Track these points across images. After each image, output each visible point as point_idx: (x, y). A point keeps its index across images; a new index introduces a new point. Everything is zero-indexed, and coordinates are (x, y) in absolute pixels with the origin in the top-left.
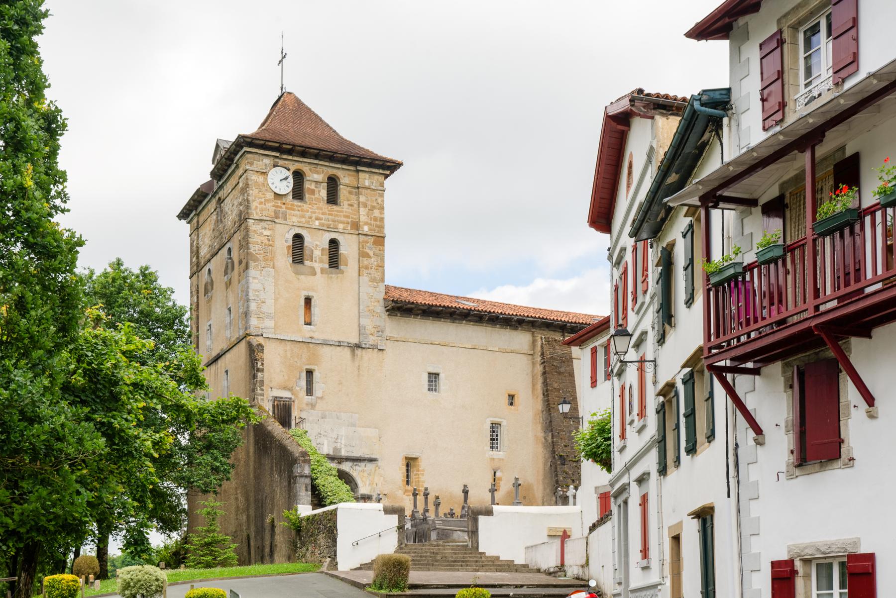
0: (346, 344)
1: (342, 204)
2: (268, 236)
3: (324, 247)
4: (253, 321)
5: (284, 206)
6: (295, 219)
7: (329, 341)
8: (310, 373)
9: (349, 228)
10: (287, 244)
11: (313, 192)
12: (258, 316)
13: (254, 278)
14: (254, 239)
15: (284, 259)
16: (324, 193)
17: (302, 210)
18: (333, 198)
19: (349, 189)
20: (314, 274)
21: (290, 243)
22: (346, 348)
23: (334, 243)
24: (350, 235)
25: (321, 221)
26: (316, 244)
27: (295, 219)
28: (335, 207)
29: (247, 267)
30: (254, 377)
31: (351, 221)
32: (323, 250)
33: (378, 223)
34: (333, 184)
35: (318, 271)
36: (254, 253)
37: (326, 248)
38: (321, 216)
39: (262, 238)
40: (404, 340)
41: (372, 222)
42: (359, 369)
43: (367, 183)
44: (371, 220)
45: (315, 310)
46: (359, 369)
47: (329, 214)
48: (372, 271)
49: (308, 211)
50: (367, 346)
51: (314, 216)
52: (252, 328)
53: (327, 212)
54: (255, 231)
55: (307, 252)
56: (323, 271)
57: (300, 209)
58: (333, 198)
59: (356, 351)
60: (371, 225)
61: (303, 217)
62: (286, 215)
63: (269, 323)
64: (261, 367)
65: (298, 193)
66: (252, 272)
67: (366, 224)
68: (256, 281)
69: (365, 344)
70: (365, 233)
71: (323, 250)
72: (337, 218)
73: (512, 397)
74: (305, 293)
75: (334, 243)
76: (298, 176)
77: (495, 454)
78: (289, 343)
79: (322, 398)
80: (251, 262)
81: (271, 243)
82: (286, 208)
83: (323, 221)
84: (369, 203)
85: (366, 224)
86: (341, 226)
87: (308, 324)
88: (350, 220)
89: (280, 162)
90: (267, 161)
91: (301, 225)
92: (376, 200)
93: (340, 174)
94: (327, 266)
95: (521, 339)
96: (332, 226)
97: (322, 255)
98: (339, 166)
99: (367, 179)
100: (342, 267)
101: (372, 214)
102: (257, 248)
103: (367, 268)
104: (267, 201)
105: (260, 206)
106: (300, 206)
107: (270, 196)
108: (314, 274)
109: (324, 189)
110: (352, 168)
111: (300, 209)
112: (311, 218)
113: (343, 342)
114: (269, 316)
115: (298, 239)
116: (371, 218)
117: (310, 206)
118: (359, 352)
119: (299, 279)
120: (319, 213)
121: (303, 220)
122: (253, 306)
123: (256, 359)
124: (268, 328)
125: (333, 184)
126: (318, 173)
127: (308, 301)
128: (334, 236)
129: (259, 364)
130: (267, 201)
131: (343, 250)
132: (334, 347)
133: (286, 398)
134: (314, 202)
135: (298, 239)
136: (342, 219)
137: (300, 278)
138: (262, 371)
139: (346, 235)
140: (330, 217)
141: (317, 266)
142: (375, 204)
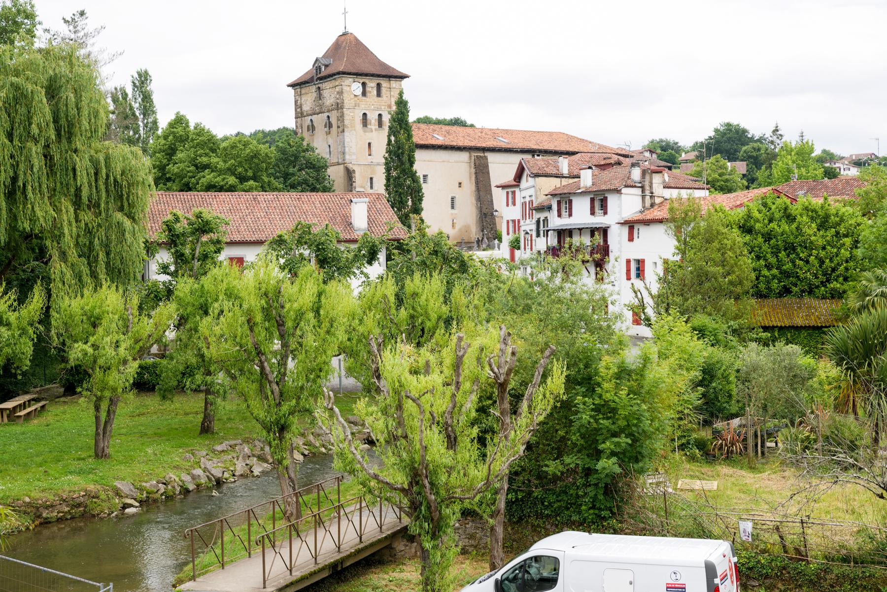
4: (347, 157)
8: (371, 179)
11: (370, 92)
14: (346, 118)
16: (375, 92)
18: (379, 94)
20: (372, 131)
23: (380, 115)
26: (373, 117)
27: (363, 106)
29: (343, 131)
30: (352, 185)
34: (379, 86)
43: (394, 86)
45: (373, 148)
56: (376, 130)
58: (379, 94)
63: (354, 157)
65: (364, 94)
66: (346, 134)
73: (460, 184)
74: (369, 141)
75: (380, 115)
76: (364, 84)
77: (453, 211)
86: (383, 107)
87: (370, 155)
89: (356, 80)
90: (351, 80)
95: (464, 156)
99: (394, 84)
104: (351, 99)
107: (352, 96)
108: (372, 131)
115: (365, 114)
122: (347, 149)
125: (379, 86)
127: (369, 144)
128: (380, 112)
130: (351, 99)
135: (365, 114)
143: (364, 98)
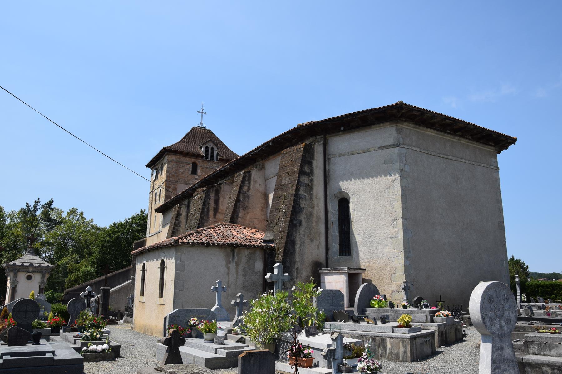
98: (161, 159)
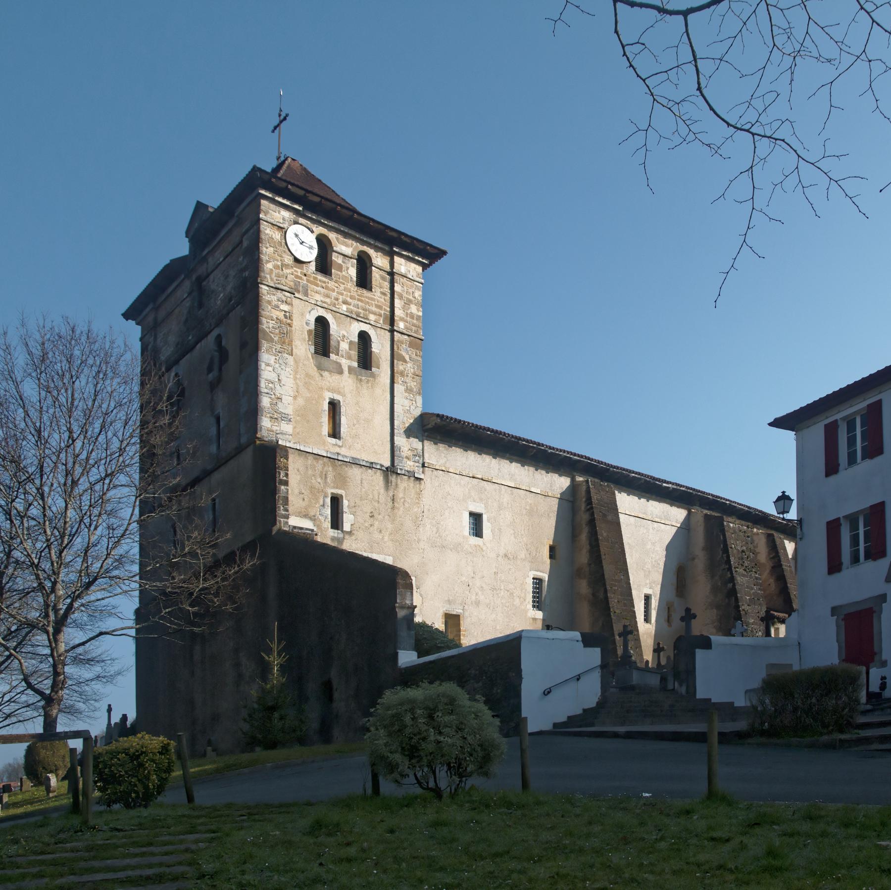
0: (378, 467)
1: (373, 290)
2: (285, 312)
3: (353, 340)
5: (305, 278)
6: (318, 297)
7: (358, 459)
9: (381, 322)
10: (308, 328)
12: (272, 415)
13: (268, 365)
15: (304, 348)
16: (353, 272)
17: (327, 288)
19: (382, 273)
20: (341, 372)
21: (312, 326)
22: (379, 471)
24: (383, 330)
25: (349, 307)
28: (365, 292)
31: (384, 313)
32: (351, 343)
33: (415, 321)
34: (364, 265)
35: (346, 369)
36: (267, 330)
37: (355, 342)
38: (349, 299)
39: (278, 313)
40: (444, 469)
41: (408, 319)
42: (393, 500)
44: (407, 316)
46: (393, 500)
47: (359, 300)
48: (408, 380)
49: (334, 290)
50: (403, 472)
51: (341, 298)
52: (263, 431)
53: (357, 297)
54: (269, 302)
55: (333, 343)
56: (351, 369)
57: (324, 285)
58: (364, 281)
59: (390, 477)
60: (407, 322)
61: (328, 296)
62: (307, 290)
63: (286, 427)
64: (285, 478)
65: (324, 265)
67: (402, 319)
68: (271, 369)
69: (401, 469)
70: (401, 330)
71: (351, 343)
72: (367, 306)
74: (328, 396)
76: (324, 245)
78: (310, 457)
79: (350, 533)
80: (263, 341)
81: (289, 321)
82: (308, 281)
83: (351, 307)
84: (405, 295)
85: (402, 319)
86: (372, 317)
88: (383, 312)
89: (301, 220)
90: (286, 214)
91: (326, 306)
92: (413, 293)
93: (371, 252)
94: (355, 364)
96: (362, 315)
97: (350, 349)
100: (373, 369)
101: (409, 308)
102: (271, 326)
103: (402, 374)
104: (287, 266)
105: (275, 271)
106: (324, 282)
108: (341, 372)
109: (353, 267)
110: (387, 248)
111: (324, 285)
112: (337, 299)
113: (375, 463)
114: (285, 418)
115: (321, 322)
116: (407, 314)
117: (337, 285)
118: (393, 478)
119: (322, 376)
120: (347, 296)
121: (328, 300)
123: (279, 467)
124: (285, 434)
125: (364, 265)
126: (347, 246)
129: (282, 474)
131: (375, 348)
132: (365, 468)
133: (307, 529)
134: (341, 280)
136: (374, 309)
137: (324, 374)
138: (286, 483)
139: (379, 329)
140: (360, 304)
141: (345, 363)
142: (411, 297)
143: (320, 277)
